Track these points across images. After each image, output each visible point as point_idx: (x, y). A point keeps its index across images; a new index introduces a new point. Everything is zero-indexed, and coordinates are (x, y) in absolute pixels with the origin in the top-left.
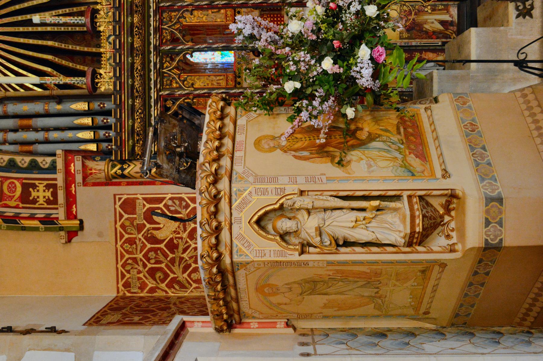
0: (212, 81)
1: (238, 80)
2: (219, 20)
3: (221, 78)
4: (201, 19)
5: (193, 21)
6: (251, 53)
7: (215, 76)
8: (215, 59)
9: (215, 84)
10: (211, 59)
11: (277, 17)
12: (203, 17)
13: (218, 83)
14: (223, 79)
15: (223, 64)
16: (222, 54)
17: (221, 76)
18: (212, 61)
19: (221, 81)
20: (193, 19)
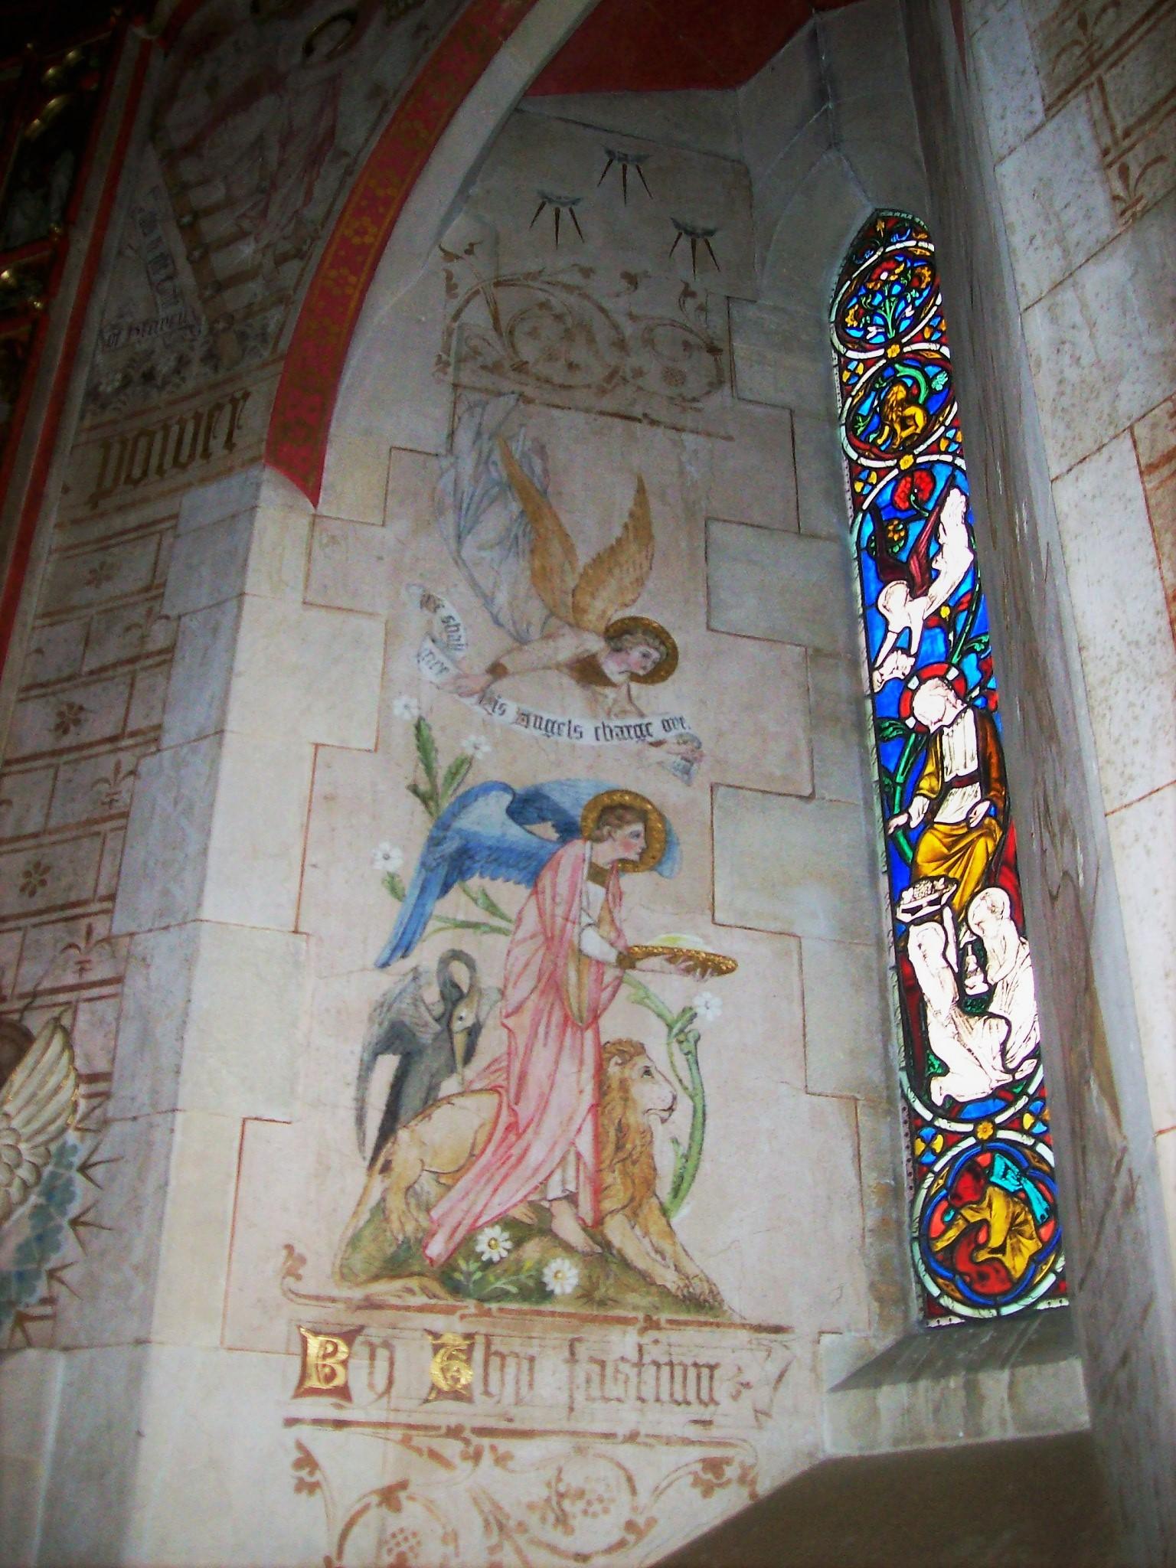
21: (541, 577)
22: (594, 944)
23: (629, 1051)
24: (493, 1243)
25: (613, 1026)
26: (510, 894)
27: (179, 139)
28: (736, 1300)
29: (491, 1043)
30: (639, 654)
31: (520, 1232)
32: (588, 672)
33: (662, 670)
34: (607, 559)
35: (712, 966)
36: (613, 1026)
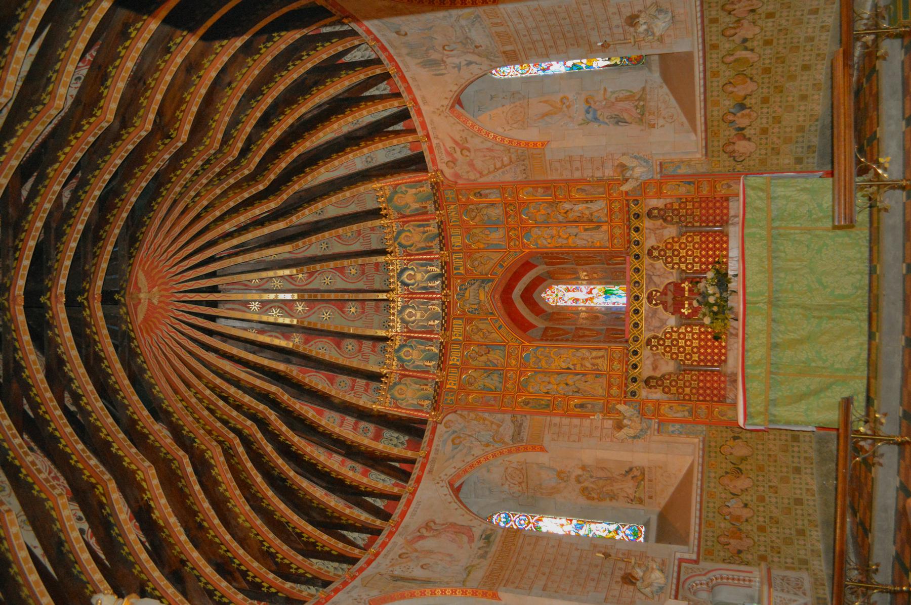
0: (583, 359)
1: (634, 360)
2: (598, 244)
3: (601, 353)
4: (565, 242)
5: (549, 246)
6: (661, 306)
7: (589, 348)
8: (595, 301)
9: (588, 365)
10: (586, 300)
11: (715, 242)
12: (567, 238)
13: (593, 365)
14: (603, 356)
15: (607, 308)
16: (606, 292)
17: (600, 349)
18: (587, 304)
19: (599, 361)
20: (549, 241)
21: (555, 113)
22: (604, 103)
23: (616, 98)
24: (639, 111)
25: (614, 100)
26: (599, 113)
27: (478, 175)
28: (643, 86)
29: (617, 113)
30: (565, 101)
31: (637, 108)
32: (568, 107)
33: (567, 98)
34: (551, 106)
35: (605, 90)
36: (614, 100)
